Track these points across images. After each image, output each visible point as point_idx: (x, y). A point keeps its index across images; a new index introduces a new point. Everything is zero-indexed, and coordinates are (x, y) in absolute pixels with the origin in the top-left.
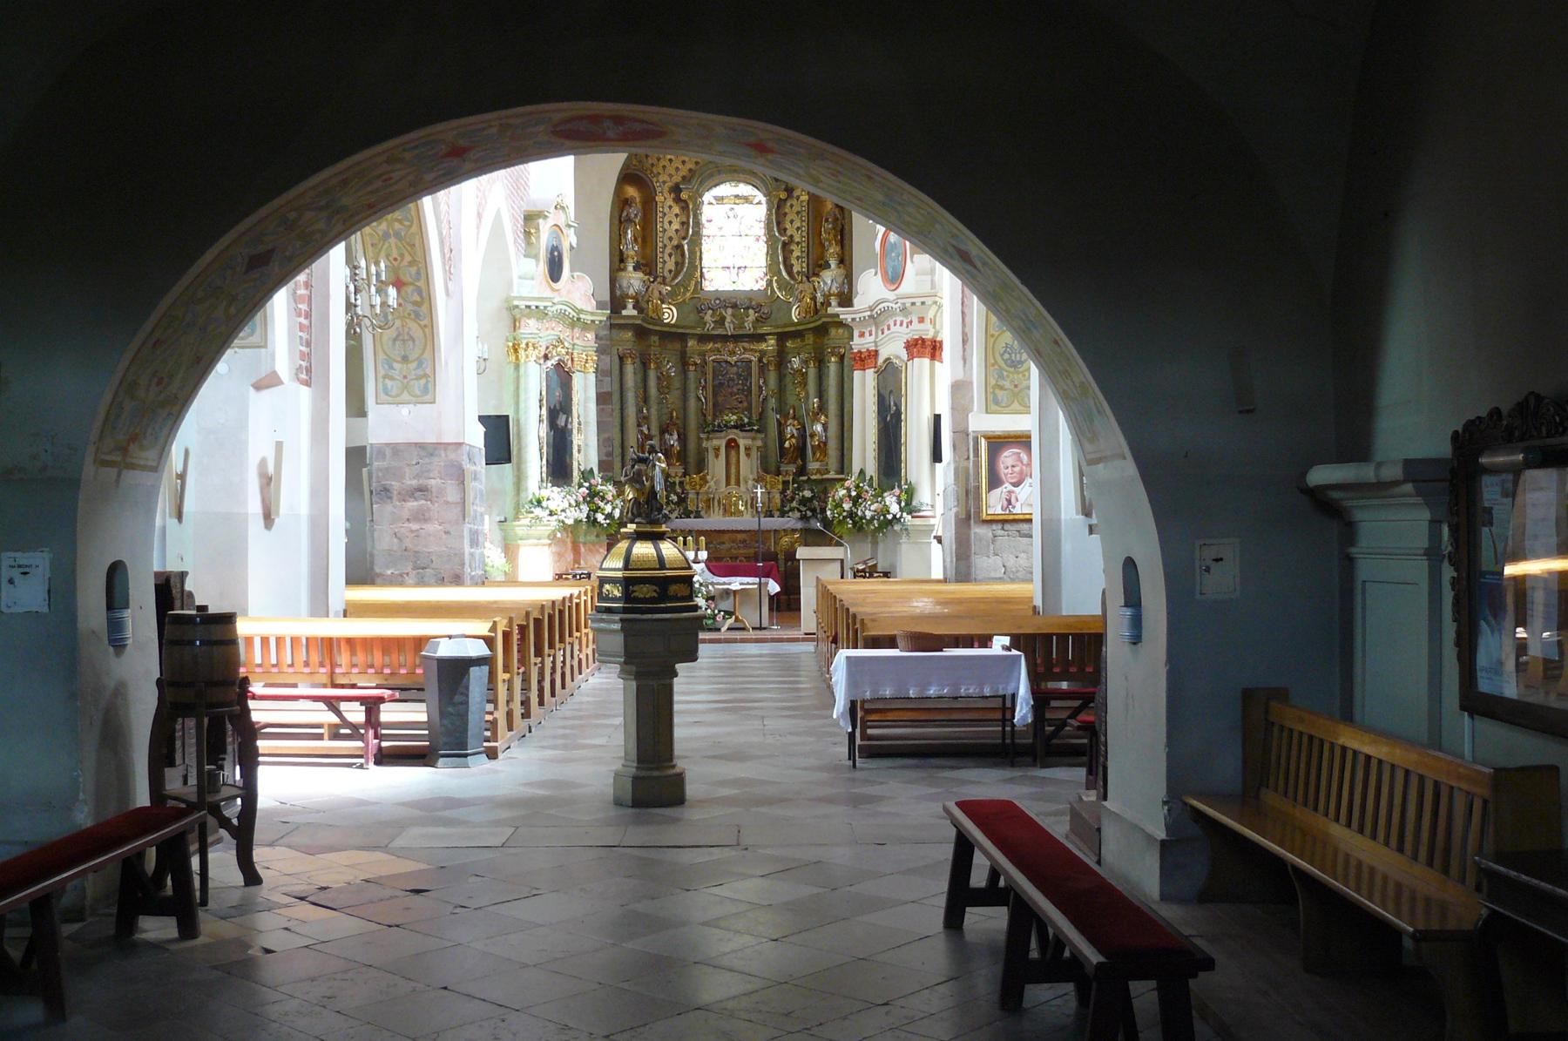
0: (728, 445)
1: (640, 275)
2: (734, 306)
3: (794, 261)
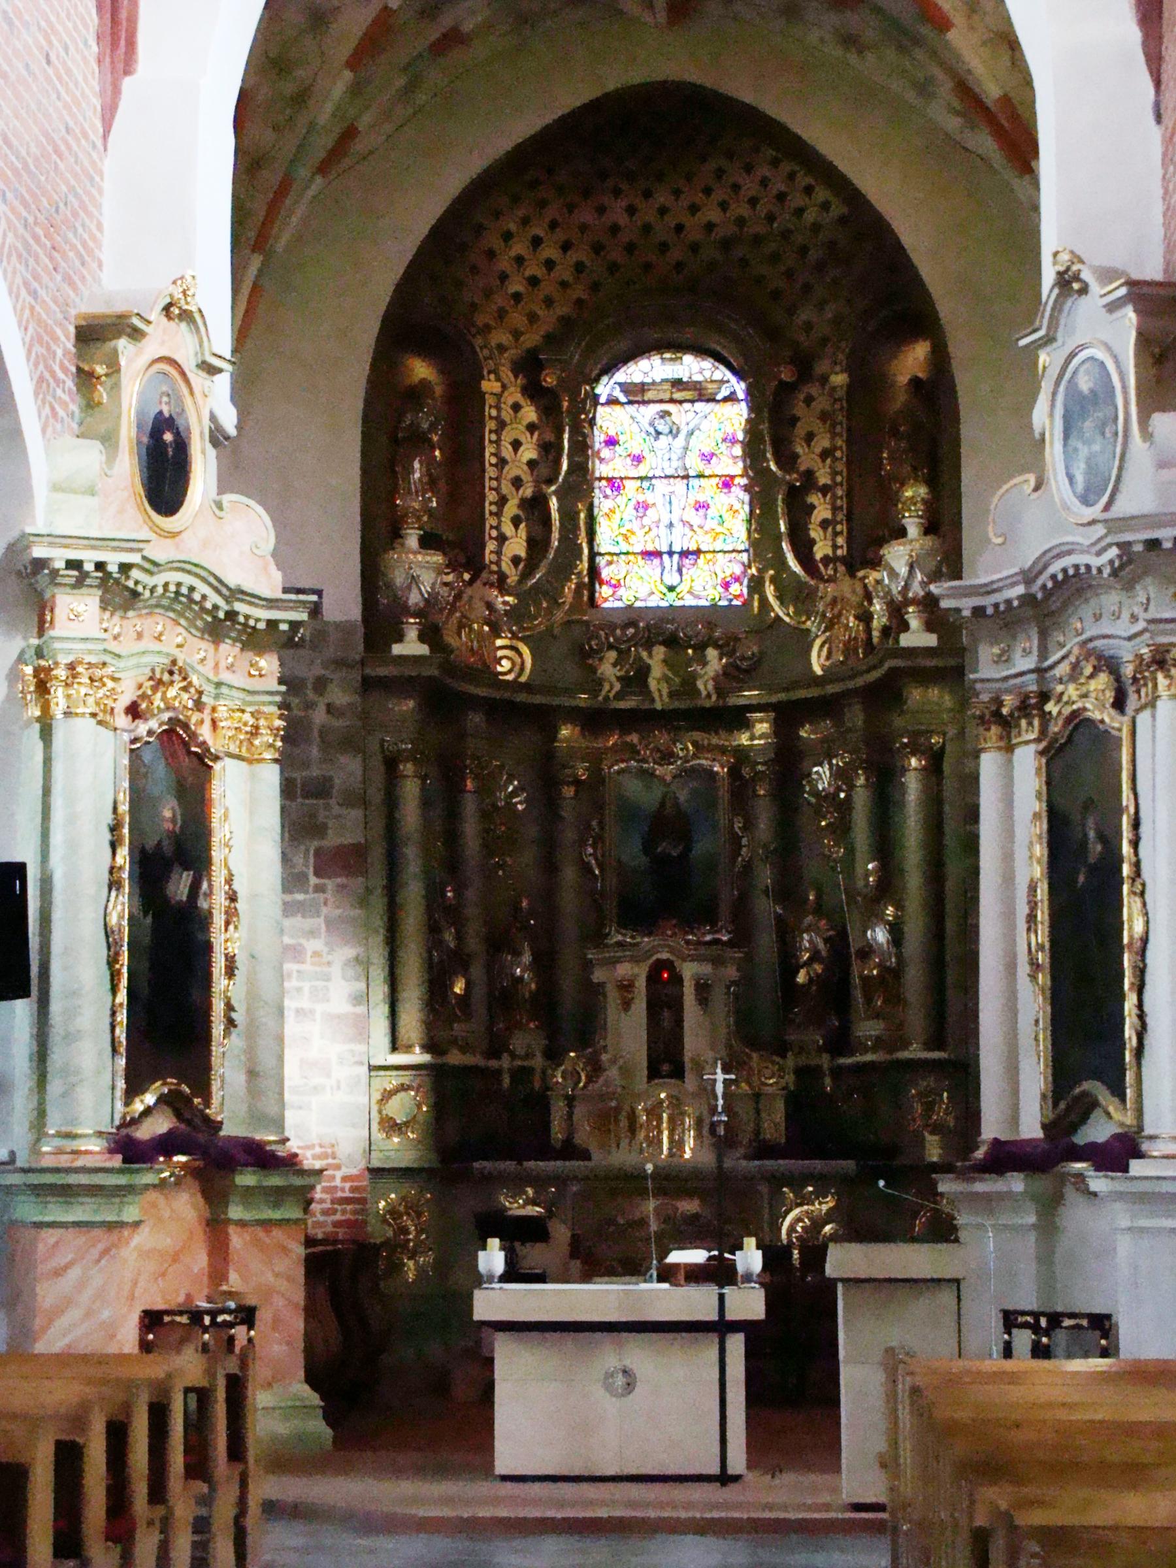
0: (653, 977)
1: (438, 558)
2: (672, 642)
3: (815, 533)
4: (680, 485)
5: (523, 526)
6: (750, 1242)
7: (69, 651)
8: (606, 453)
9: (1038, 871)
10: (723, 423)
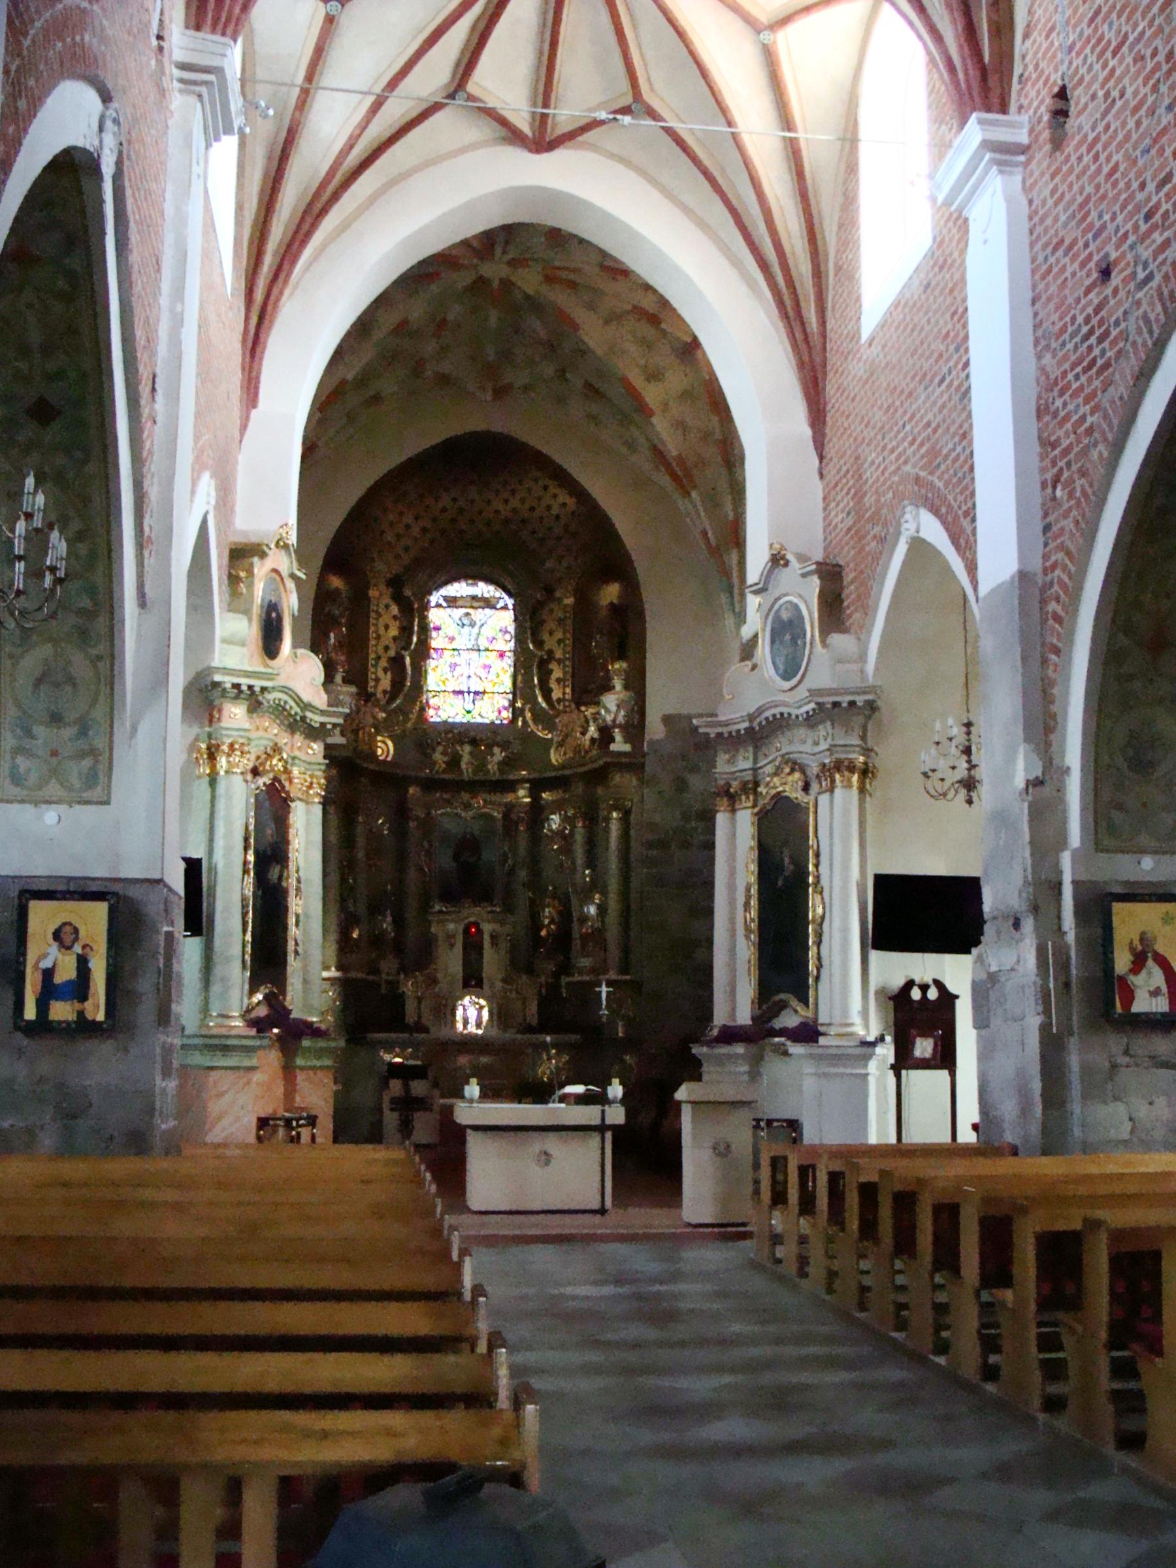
0: (466, 931)
2: (474, 742)
3: (553, 685)
4: (475, 654)
5: (389, 673)
6: (616, 1081)
7: (229, 736)
8: (434, 634)
9: (753, 879)
10: (500, 623)
